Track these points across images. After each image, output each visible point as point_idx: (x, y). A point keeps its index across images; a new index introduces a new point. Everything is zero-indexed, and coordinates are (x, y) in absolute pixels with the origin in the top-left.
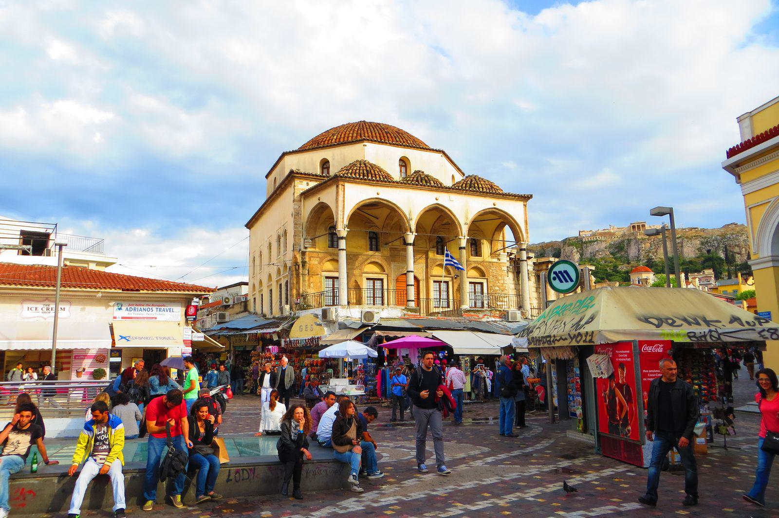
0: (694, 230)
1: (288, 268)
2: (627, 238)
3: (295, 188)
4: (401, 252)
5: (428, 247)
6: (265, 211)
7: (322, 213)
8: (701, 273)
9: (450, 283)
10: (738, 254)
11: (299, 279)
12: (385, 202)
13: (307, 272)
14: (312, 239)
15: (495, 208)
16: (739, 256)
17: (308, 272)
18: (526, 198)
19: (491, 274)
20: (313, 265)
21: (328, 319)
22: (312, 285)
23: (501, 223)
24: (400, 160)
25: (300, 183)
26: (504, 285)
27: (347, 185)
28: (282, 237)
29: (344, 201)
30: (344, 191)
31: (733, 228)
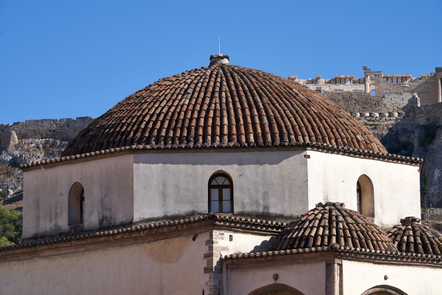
3: (214, 245)
6: (46, 253)
24: (358, 181)
25: (220, 236)
27: (346, 264)
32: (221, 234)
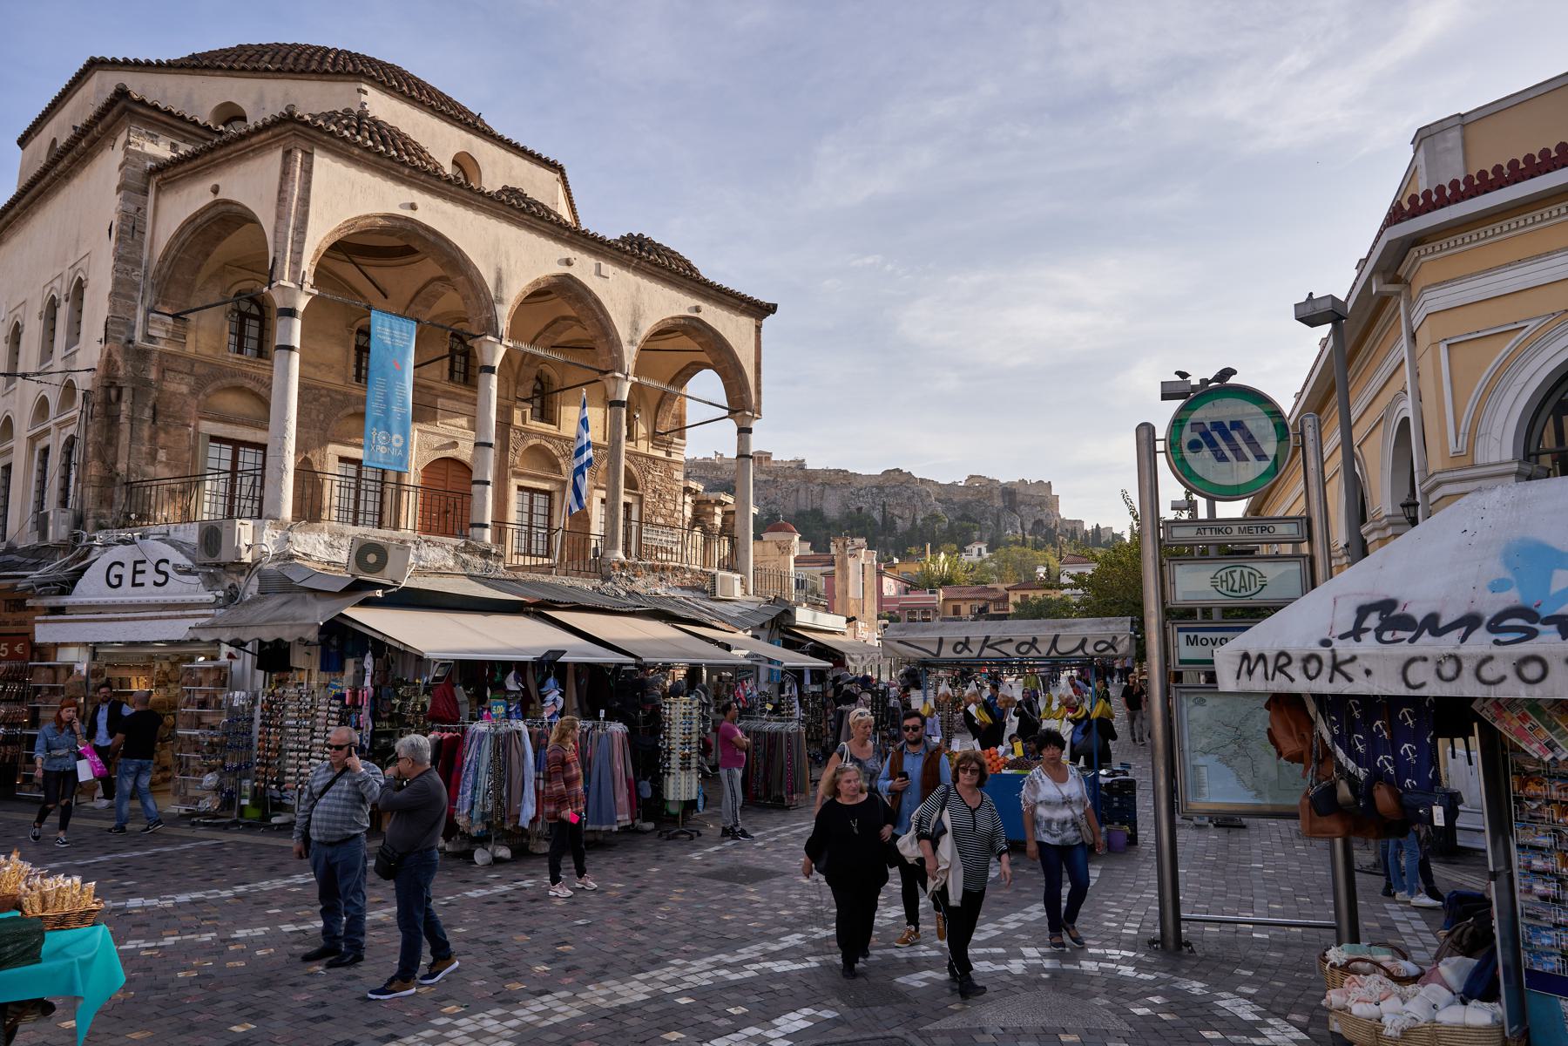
1: (79, 394)
4: (440, 401)
5: (511, 396)
7: (219, 238)
9: (557, 496)
11: (118, 432)
12: (432, 238)
13: (148, 413)
14: (175, 316)
15: (698, 320)
17: (154, 414)
18: (760, 310)
19: (649, 485)
20: (174, 394)
21: (225, 556)
22: (162, 455)
23: (688, 366)
24: (454, 162)
26: (676, 515)
28: (63, 302)
29: (305, 200)
30: (308, 171)
32: (151, 135)
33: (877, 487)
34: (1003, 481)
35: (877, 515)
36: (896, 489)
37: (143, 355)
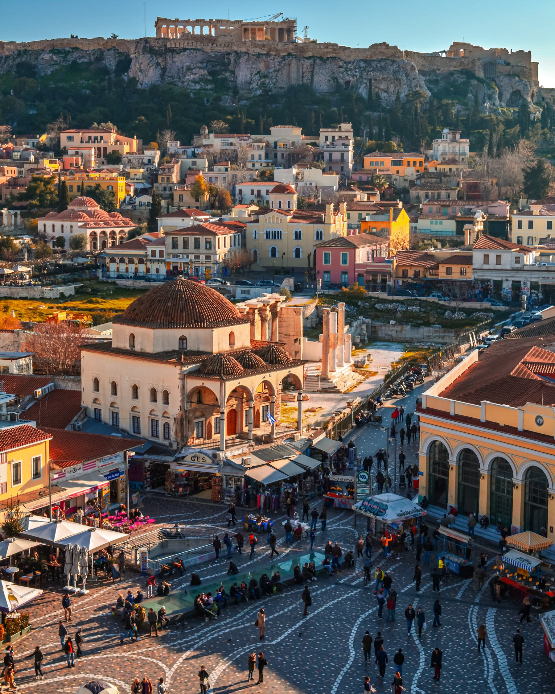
0: (331, 47)
2: (235, 48)
8: (337, 130)
10: (385, 92)
16: (385, 94)
31: (382, 50)
33: (365, 61)
34: (486, 48)
35: (363, 91)
36: (383, 64)
37: (186, 411)
